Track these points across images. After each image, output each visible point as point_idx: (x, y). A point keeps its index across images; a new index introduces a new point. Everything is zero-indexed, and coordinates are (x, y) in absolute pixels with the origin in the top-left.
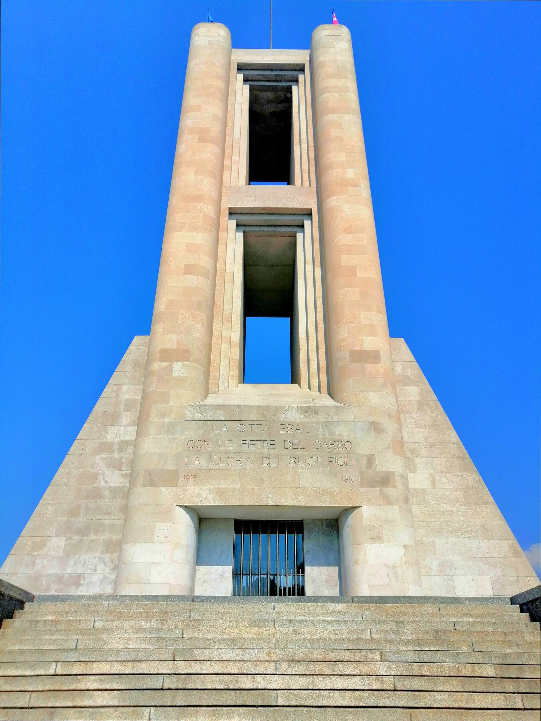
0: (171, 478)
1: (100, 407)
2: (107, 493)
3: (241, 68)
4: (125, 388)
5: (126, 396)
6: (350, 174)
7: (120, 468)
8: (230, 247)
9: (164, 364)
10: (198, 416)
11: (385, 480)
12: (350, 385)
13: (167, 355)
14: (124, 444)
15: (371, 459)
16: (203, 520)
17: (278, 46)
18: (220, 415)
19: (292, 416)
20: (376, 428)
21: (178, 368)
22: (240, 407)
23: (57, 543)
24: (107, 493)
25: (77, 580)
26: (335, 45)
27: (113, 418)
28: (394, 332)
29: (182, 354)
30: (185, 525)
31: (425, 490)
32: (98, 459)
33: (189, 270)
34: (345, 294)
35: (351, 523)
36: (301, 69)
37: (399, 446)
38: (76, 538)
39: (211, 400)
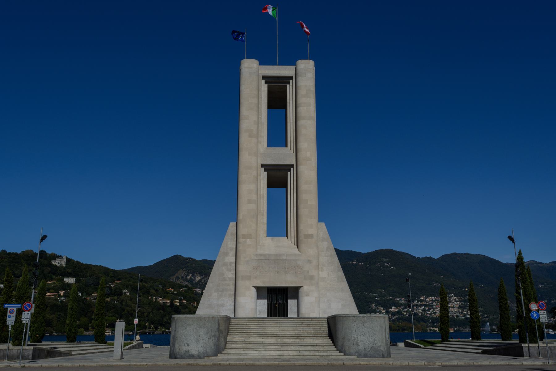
0: (249, 278)
1: (222, 250)
2: (228, 279)
3: (264, 78)
4: (229, 243)
5: (230, 246)
6: (308, 154)
7: (231, 271)
8: (262, 182)
9: (244, 240)
10: (256, 258)
11: (312, 278)
12: (303, 246)
13: (244, 236)
14: (231, 263)
15: (308, 272)
16: (258, 289)
17: (281, 64)
18: (262, 258)
19: (284, 258)
20: (310, 262)
21: (248, 241)
22: (269, 255)
23: (215, 294)
24: (228, 279)
25: (222, 305)
26: (306, 68)
27: (226, 254)
28: (320, 220)
29: (249, 236)
30: (254, 291)
31: (325, 278)
32: (223, 268)
33: (249, 202)
34: (303, 211)
35: (301, 290)
36: (291, 78)
37: (318, 267)
38: (220, 293)
39: (259, 252)
